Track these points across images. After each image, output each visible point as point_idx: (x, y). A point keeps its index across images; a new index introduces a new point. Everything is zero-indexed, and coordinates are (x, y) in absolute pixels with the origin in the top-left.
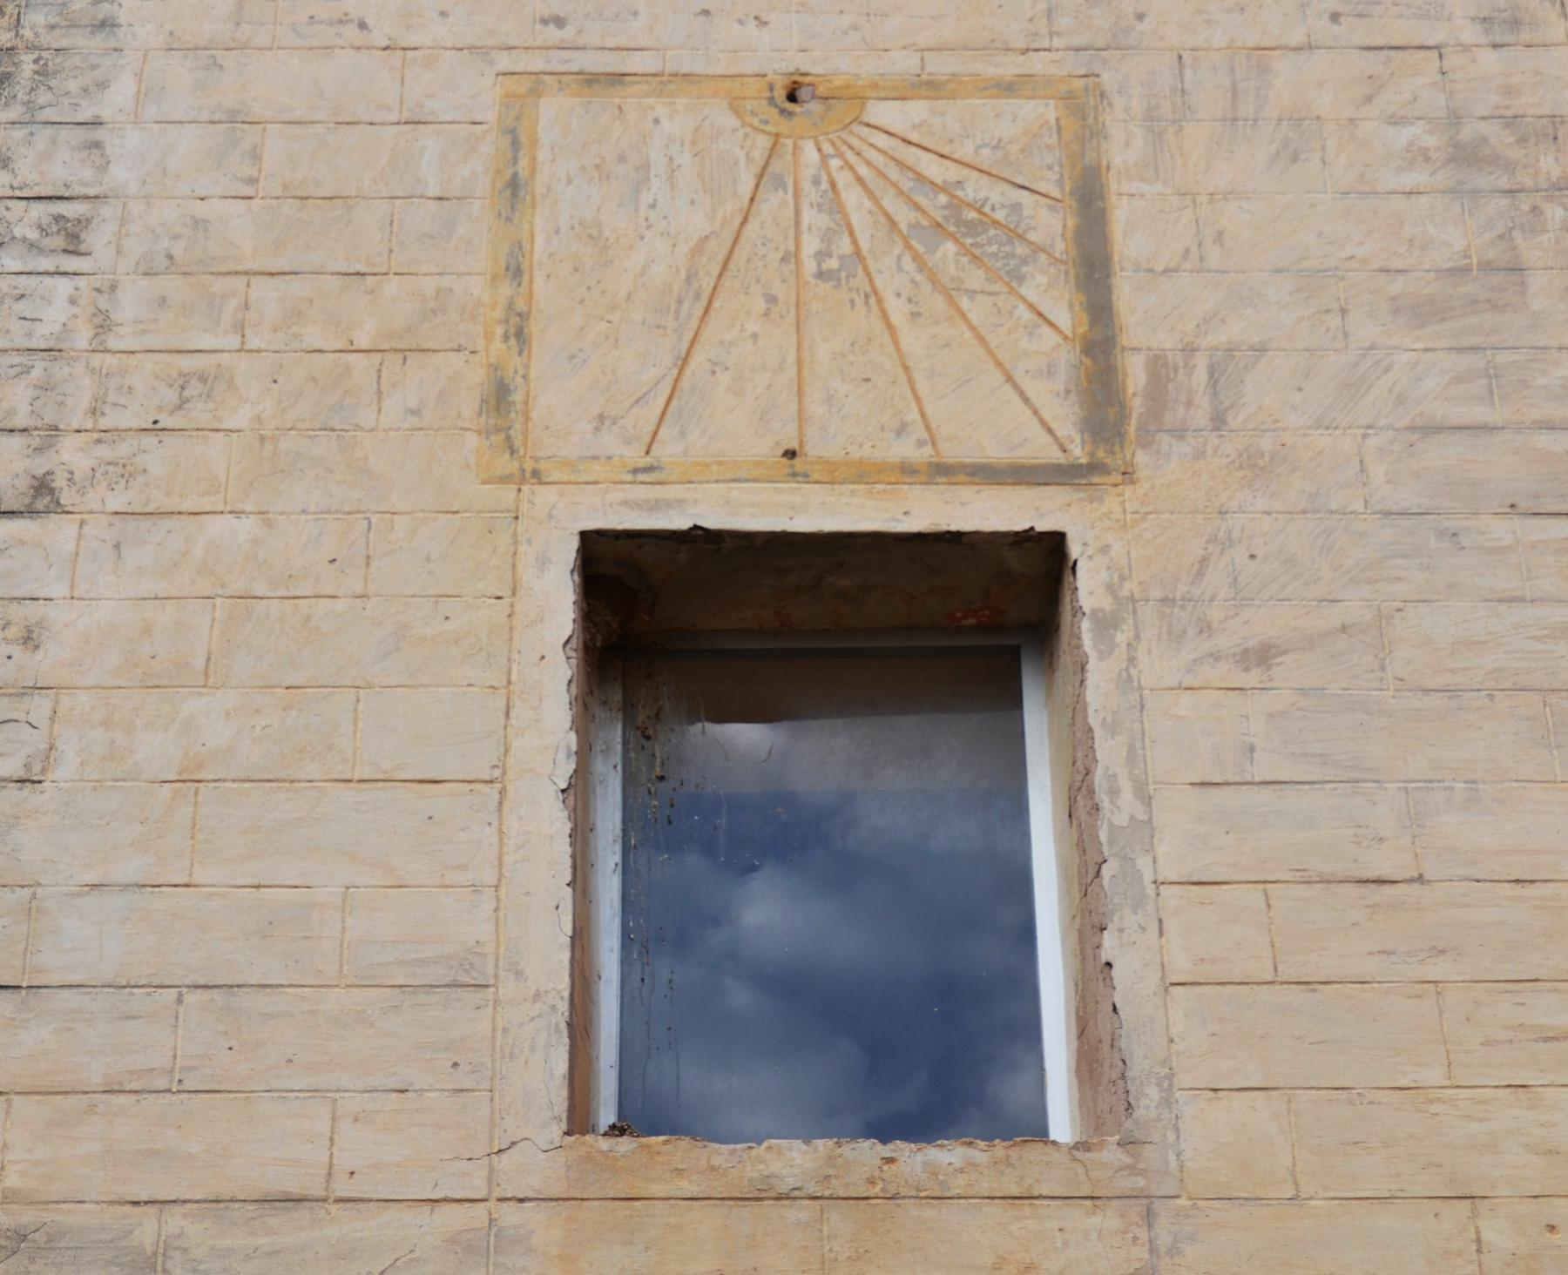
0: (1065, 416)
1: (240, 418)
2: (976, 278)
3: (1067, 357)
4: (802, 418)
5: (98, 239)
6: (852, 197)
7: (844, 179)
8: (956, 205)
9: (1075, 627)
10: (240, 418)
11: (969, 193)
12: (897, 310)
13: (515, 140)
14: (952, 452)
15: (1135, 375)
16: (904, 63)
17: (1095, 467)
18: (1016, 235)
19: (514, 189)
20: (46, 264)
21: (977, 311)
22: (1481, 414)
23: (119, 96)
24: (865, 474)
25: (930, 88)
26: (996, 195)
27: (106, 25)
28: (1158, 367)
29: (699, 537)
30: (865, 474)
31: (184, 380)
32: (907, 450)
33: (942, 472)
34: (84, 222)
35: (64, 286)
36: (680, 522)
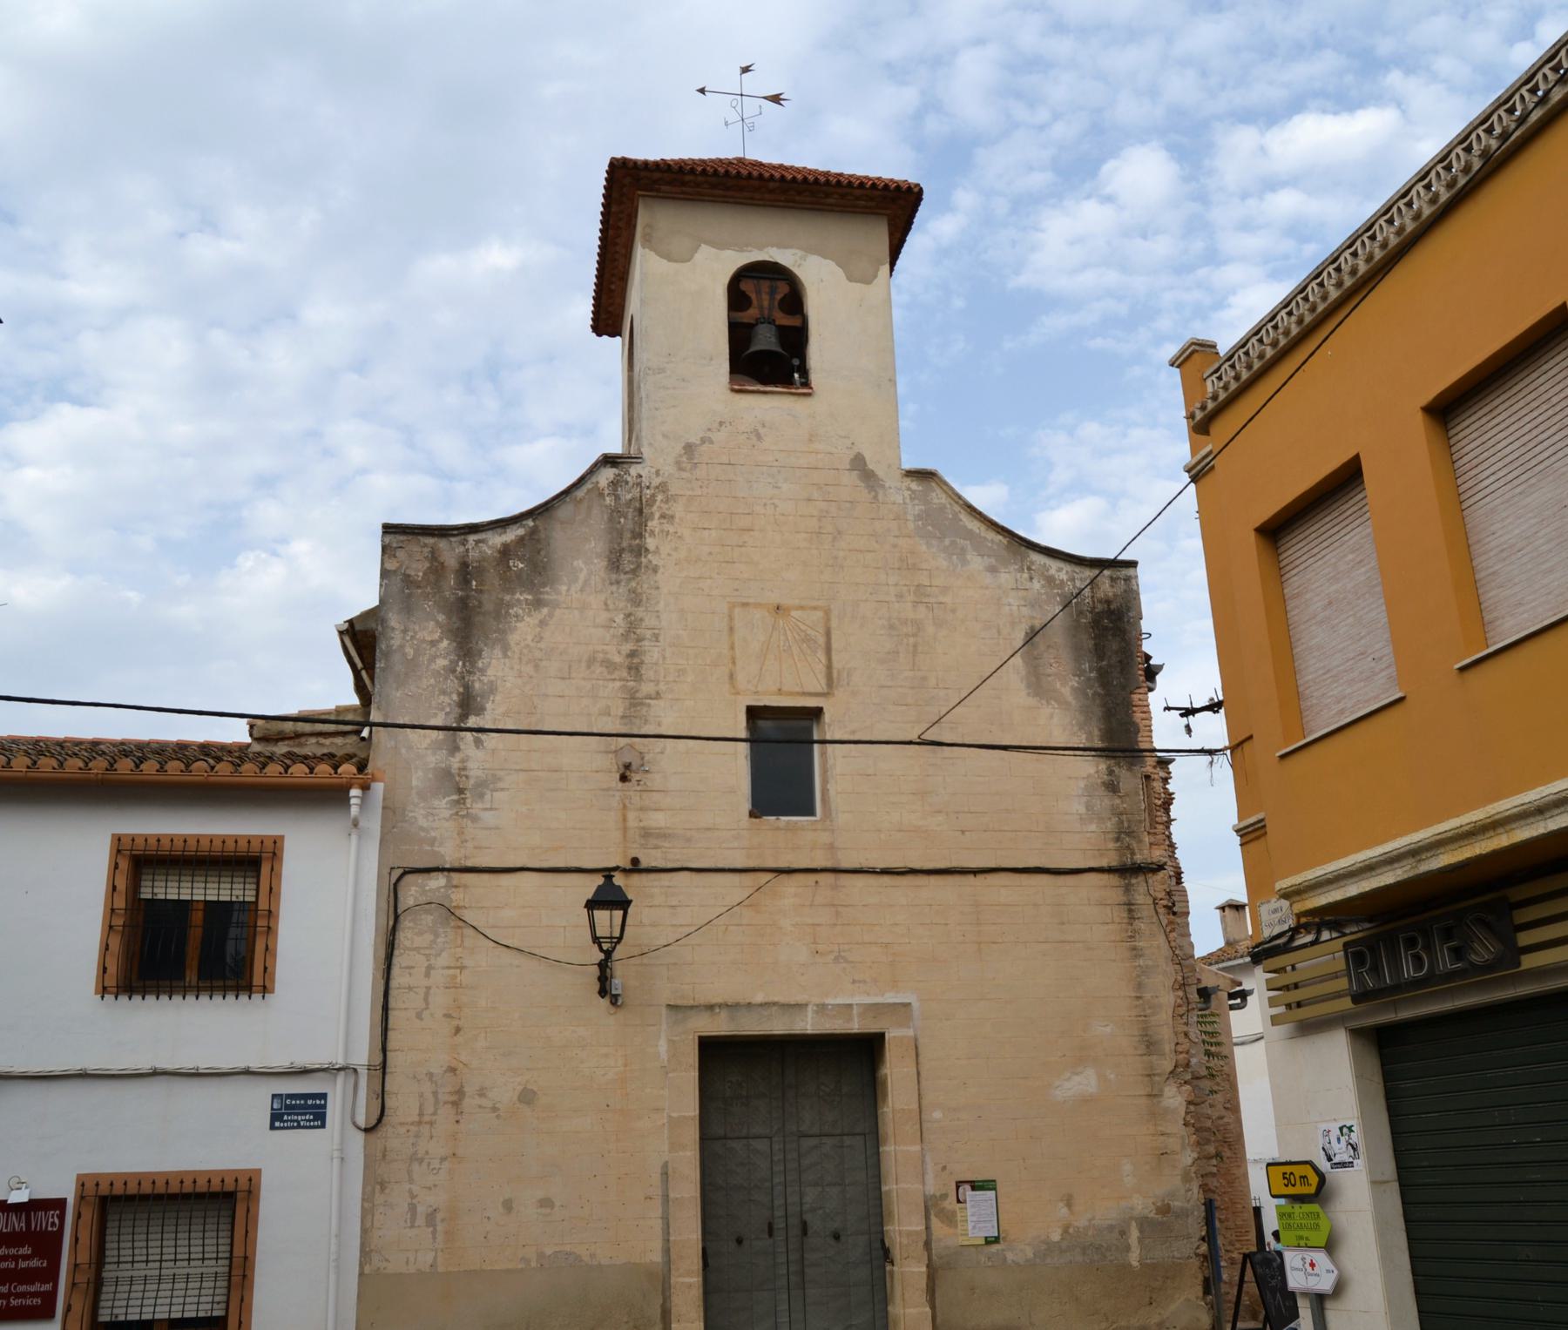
0: (823, 682)
1: (689, 680)
2: (809, 652)
3: (824, 669)
4: (781, 682)
5: (661, 638)
6: (788, 632)
7: (787, 628)
8: (806, 635)
9: (824, 726)
10: (689, 680)
11: (808, 632)
12: (796, 658)
13: (731, 618)
14: (805, 690)
15: (835, 675)
16: (797, 602)
17: (828, 693)
18: (815, 642)
19: (731, 629)
20: (653, 644)
21: (809, 659)
22: (889, 684)
23: (661, 606)
24: (791, 694)
25: (802, 608)
26: (813, 633)
27: (658, 588)
28: (839, 672)
29: (765, 707)
30: (791, 694)
31: (679, 670)
32: (798, 689)
33: (804, 694)
34: (658, 634)
35: (656, 649)
36: (761, 704)
